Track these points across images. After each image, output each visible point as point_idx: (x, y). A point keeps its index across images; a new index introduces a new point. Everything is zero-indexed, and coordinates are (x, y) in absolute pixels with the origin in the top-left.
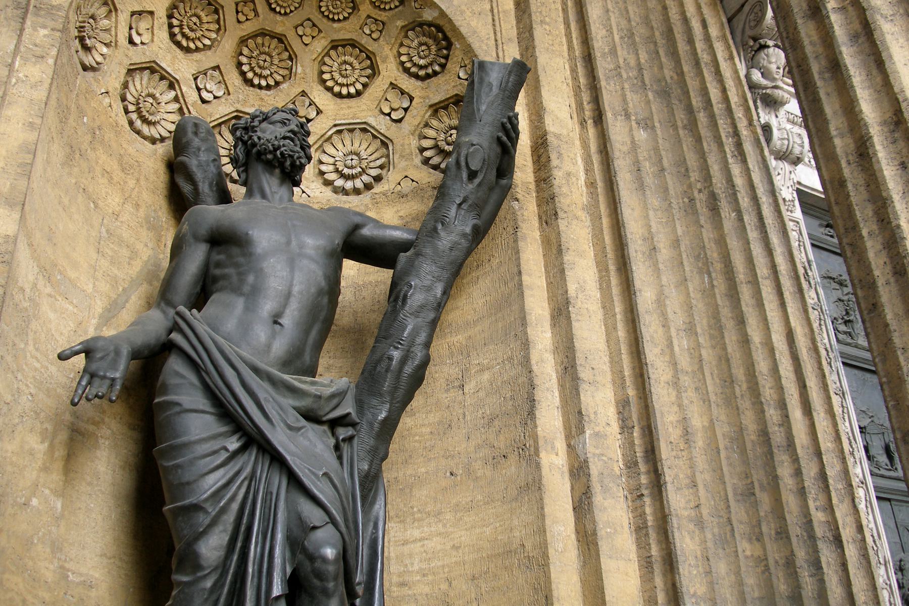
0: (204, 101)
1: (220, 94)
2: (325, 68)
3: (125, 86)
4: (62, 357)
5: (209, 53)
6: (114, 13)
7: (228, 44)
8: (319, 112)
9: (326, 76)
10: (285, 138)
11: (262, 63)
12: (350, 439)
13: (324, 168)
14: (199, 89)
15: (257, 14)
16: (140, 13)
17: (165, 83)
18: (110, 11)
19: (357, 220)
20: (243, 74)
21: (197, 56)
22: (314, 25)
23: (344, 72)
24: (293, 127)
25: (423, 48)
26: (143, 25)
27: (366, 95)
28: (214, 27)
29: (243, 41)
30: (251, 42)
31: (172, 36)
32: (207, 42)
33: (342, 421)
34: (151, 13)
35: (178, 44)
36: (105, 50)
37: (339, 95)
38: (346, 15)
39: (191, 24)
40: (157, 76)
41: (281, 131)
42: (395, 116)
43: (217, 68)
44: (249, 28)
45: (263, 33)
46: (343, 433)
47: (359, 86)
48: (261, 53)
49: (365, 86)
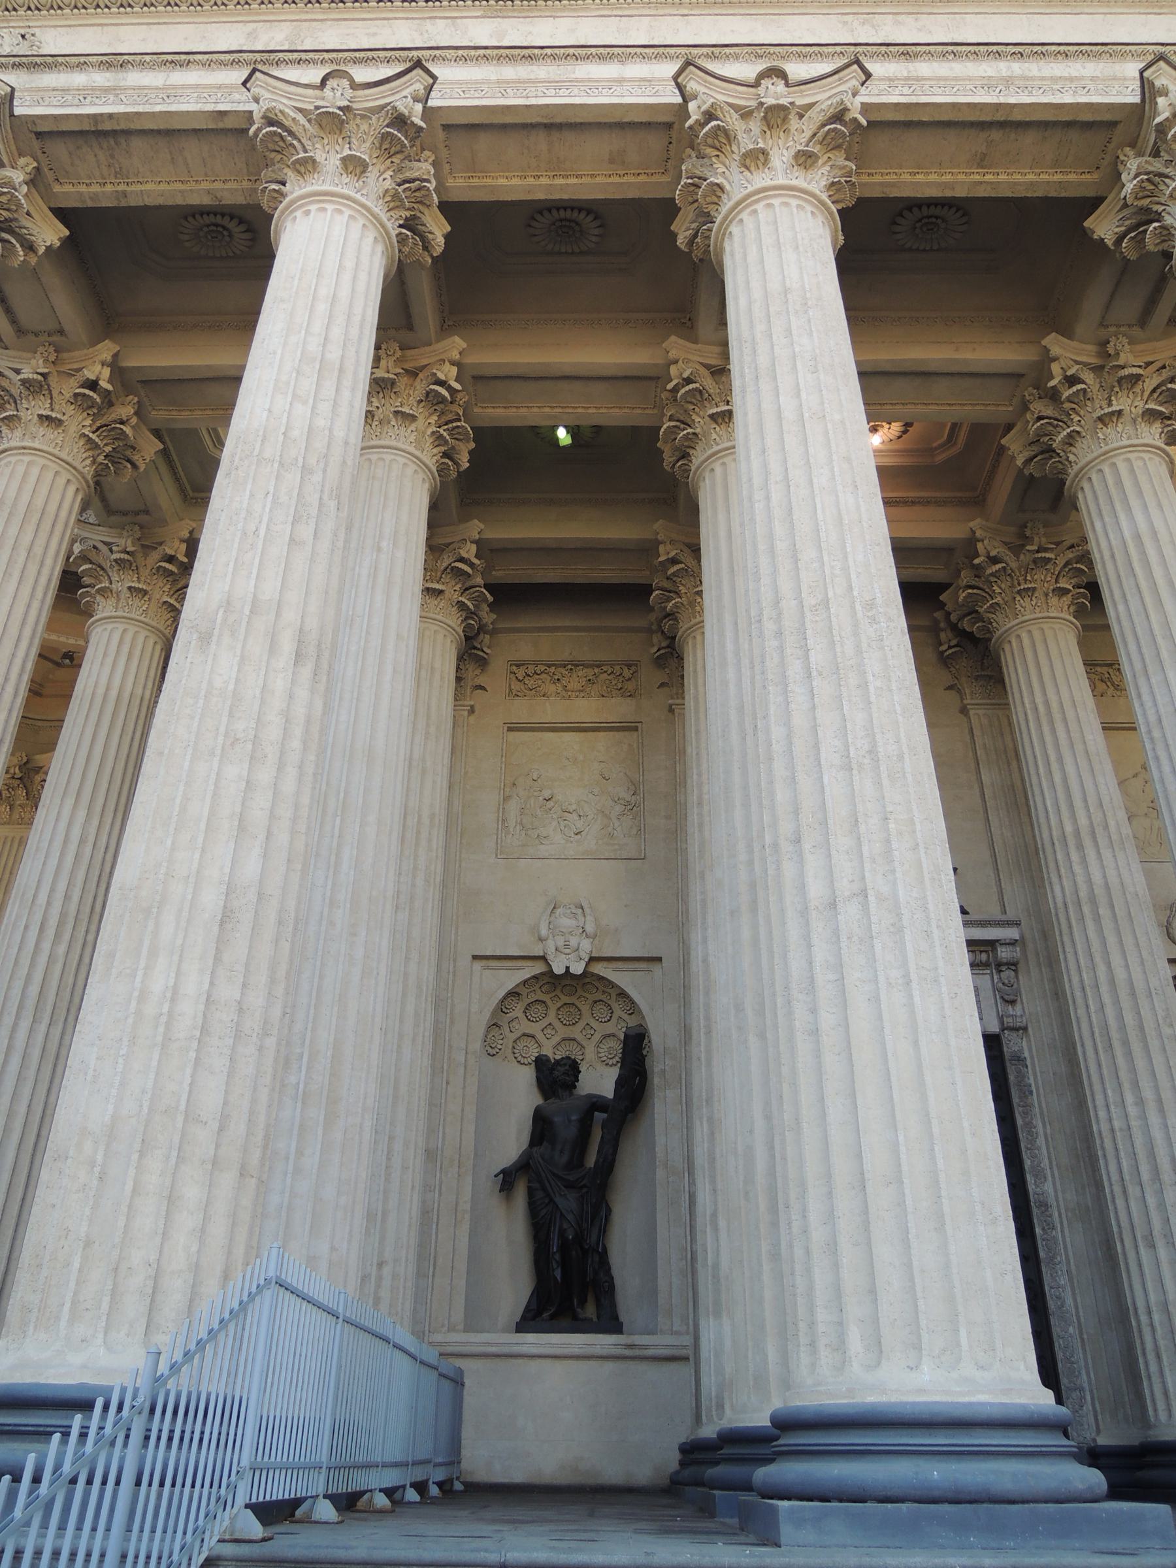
1: (553, 1032)
3: (514, 1048)
4: (496, 1176)
7: (552, 1013)
10: (564, 1073)
12: (587, 1192)
13: (600, 1055)
19: (595, 1100)
24: (567, 1067)
26: (514, 1024)
29: (559, 1009)
31: (529, 1020)
33: (585, 1186)
36: (501, 1042)
41: (562, 1069)
43: (550, 1024)
44: (559, 1005)
45: (565, 1004)
46: (585, 1190)
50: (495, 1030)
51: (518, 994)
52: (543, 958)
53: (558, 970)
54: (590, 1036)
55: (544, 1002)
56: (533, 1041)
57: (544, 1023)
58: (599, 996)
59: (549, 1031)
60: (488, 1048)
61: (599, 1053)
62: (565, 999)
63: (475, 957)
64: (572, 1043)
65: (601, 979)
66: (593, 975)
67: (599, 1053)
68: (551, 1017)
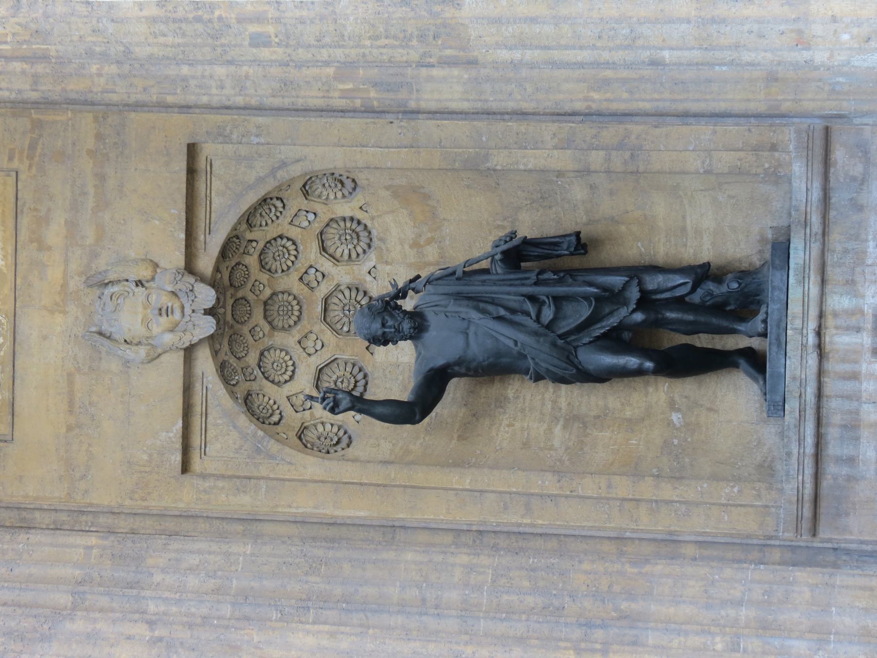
0: (323, 346)
5: (289, 350)
6: (305, 425)
7: (279, 339)
8: (311, 267)
11: (285, 312)
14: (317, 351)
16: (292, 406)
18: (305, 428)
20: (295, 323)
21: (295, 358)
25: (264, 213)
27: (293, 237)
28: (272, 351)
31: (291, 377)
32: (283, 353)
34: (287, 397)
36: (328, 427)
38: (244, 267)
39: (279, 368)
45: (265, 317)
47: (290, 243)
48: (279, 315)
49: (288, 239)
50: (311, 436)
51: (249, 394)
52: (189, 352)
53: (208, 326)
54: (319, 275)
55: (262, 354)
56: (327, 370)
57: (297, 352)
58: (252, 261)
59: (309, 343)
60: (339, 448)
63: (185, 467)
64: (332, 307)
65: (224, 253)
66: (217, 269)
68: (290, 340)
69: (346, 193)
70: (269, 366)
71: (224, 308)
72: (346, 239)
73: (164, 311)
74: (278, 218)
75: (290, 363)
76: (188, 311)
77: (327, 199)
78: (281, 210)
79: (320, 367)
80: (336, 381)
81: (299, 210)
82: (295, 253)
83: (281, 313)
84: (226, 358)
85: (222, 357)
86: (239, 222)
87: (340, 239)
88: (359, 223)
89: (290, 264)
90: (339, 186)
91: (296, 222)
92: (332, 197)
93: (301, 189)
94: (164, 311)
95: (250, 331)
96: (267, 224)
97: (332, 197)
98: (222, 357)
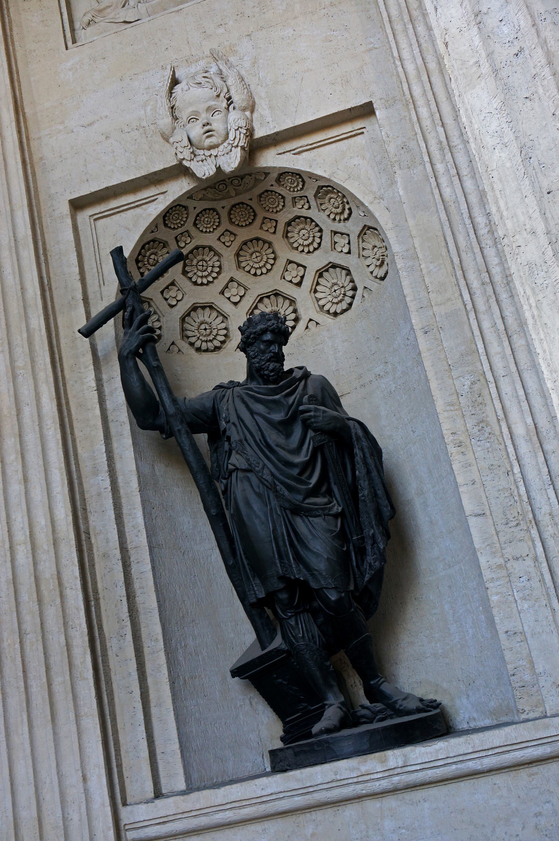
0: (236, 304)
2: (292, 240)
6: (151, 302)
9: (295, 245)
11: (256, 260)
13: (321, 303)
15: (235, 235)
17: (208, 309)
18: (149, 303)
22: (271, 220)
23: (304, 238)
30: (242, 253)
35: (202, 284)
37: (309, 252)
39: (200, 268)
40: (200, 311)
42: (346, 250)
43: (232, 280)
45: (245, 243)
48: (252, 255)
49: (321, 237)
61: (318, 300)
62: (244, 234)
66: (266, 172)
67: (318, 300)
69: (374, 274)
70: (200, 257)
71: (236, 195)
72: (335, 291)
73: (207, 128)
74: (334, 219)
75: (210, 279)
76: (214, 152)
77: (366, 258)
78: (342, 218)
79: (213, 305)
80: (206, 323)
81: (348, 235)
82: (311, 249)
83: (254, 256)
84: (191, 209)
85: (191, 204)
86: (318, 178)
87: (335, 284)
88: (353, 297)
89: (300, 248)
90: (378, 263)
91: (337, 238)
92: (368, 262)
93: (365, 226)
94: (207, 128)
95: (227, 230)
96: (324, 210)
97: (368, 262)
98: (191, 204)
